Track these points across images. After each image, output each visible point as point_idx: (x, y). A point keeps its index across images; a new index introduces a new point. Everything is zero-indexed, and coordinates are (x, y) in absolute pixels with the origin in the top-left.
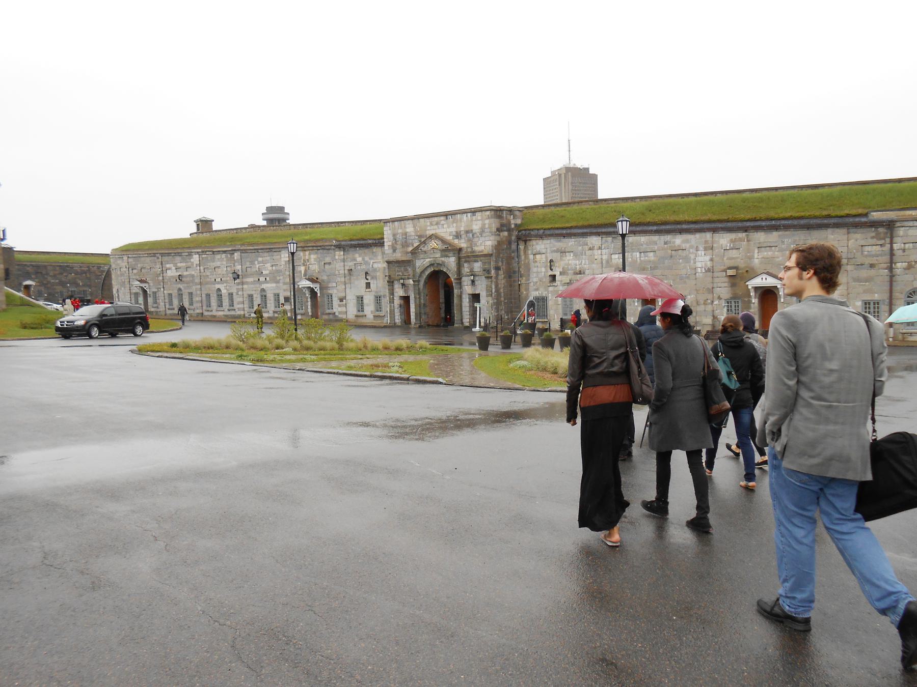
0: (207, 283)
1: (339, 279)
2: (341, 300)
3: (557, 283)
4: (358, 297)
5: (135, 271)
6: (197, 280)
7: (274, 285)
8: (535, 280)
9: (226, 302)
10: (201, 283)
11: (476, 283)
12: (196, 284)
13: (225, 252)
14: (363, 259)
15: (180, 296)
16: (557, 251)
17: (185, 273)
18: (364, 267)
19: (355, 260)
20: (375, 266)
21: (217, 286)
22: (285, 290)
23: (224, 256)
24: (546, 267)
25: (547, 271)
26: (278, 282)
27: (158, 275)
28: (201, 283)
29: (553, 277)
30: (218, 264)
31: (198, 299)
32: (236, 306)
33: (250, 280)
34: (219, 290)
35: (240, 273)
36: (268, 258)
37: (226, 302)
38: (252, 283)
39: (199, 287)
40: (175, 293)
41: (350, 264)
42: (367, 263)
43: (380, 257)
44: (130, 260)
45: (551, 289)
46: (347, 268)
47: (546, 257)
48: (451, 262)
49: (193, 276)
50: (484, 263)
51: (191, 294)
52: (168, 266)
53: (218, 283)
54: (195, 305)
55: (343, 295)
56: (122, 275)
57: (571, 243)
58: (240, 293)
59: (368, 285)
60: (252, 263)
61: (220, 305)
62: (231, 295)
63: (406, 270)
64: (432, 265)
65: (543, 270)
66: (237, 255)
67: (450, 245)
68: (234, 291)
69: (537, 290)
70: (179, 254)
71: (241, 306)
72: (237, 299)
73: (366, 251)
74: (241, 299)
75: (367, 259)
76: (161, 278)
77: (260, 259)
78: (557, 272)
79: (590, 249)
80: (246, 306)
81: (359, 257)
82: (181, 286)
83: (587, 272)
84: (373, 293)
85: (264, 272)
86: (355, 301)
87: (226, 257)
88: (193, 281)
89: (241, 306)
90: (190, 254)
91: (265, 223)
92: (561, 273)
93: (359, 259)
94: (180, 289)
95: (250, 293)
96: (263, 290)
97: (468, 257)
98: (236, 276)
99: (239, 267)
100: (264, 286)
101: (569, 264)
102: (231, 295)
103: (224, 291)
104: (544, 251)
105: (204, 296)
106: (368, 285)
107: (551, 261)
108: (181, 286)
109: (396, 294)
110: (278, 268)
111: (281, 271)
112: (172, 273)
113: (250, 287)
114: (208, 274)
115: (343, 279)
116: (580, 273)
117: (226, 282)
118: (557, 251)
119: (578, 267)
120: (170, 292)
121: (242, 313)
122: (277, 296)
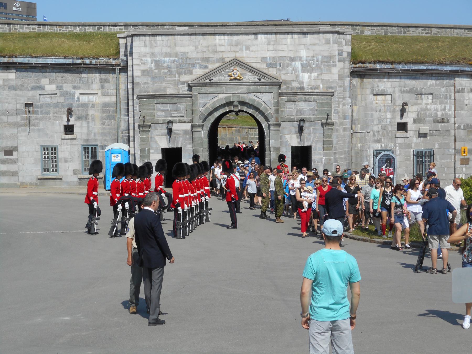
2: (8, 152)
3: (410, 133)
4: (45, 148)
8: (375, 128)
11: (305, 131)
16: (410, 91)
18: (61, 100)
19: (42, 88)
20: (84, 99)
24: (393, 112)
25: (393, 118)
29: (402, 127)
41: (30, 95)
42: (65, 94)
43: (96, 87)
45: (399, 141)
47: (393, 100)
48: (266, 100)
50: (322, 105)
57: (430, 83)
59: (69, 129)
63: (177, 109)
64: (230, 103)
65: (389, 115)
67: (265, 75)
69: (379, 141)
73: (67, 75)
75: (67, 87)
78: (408, 119)
79: (459, 92)
81: (49, 83)
83: (452, 120)
86: (39, 154)
92: (415, 121)
93: (50, 88)
97: (295, 94)
101: (426, 109)
104: (390, 91)
106: (69, 129)
107: (405, 104)
109: (154, 146)
116: (443, 121)
118: (410, 91)
119: (439, 114)
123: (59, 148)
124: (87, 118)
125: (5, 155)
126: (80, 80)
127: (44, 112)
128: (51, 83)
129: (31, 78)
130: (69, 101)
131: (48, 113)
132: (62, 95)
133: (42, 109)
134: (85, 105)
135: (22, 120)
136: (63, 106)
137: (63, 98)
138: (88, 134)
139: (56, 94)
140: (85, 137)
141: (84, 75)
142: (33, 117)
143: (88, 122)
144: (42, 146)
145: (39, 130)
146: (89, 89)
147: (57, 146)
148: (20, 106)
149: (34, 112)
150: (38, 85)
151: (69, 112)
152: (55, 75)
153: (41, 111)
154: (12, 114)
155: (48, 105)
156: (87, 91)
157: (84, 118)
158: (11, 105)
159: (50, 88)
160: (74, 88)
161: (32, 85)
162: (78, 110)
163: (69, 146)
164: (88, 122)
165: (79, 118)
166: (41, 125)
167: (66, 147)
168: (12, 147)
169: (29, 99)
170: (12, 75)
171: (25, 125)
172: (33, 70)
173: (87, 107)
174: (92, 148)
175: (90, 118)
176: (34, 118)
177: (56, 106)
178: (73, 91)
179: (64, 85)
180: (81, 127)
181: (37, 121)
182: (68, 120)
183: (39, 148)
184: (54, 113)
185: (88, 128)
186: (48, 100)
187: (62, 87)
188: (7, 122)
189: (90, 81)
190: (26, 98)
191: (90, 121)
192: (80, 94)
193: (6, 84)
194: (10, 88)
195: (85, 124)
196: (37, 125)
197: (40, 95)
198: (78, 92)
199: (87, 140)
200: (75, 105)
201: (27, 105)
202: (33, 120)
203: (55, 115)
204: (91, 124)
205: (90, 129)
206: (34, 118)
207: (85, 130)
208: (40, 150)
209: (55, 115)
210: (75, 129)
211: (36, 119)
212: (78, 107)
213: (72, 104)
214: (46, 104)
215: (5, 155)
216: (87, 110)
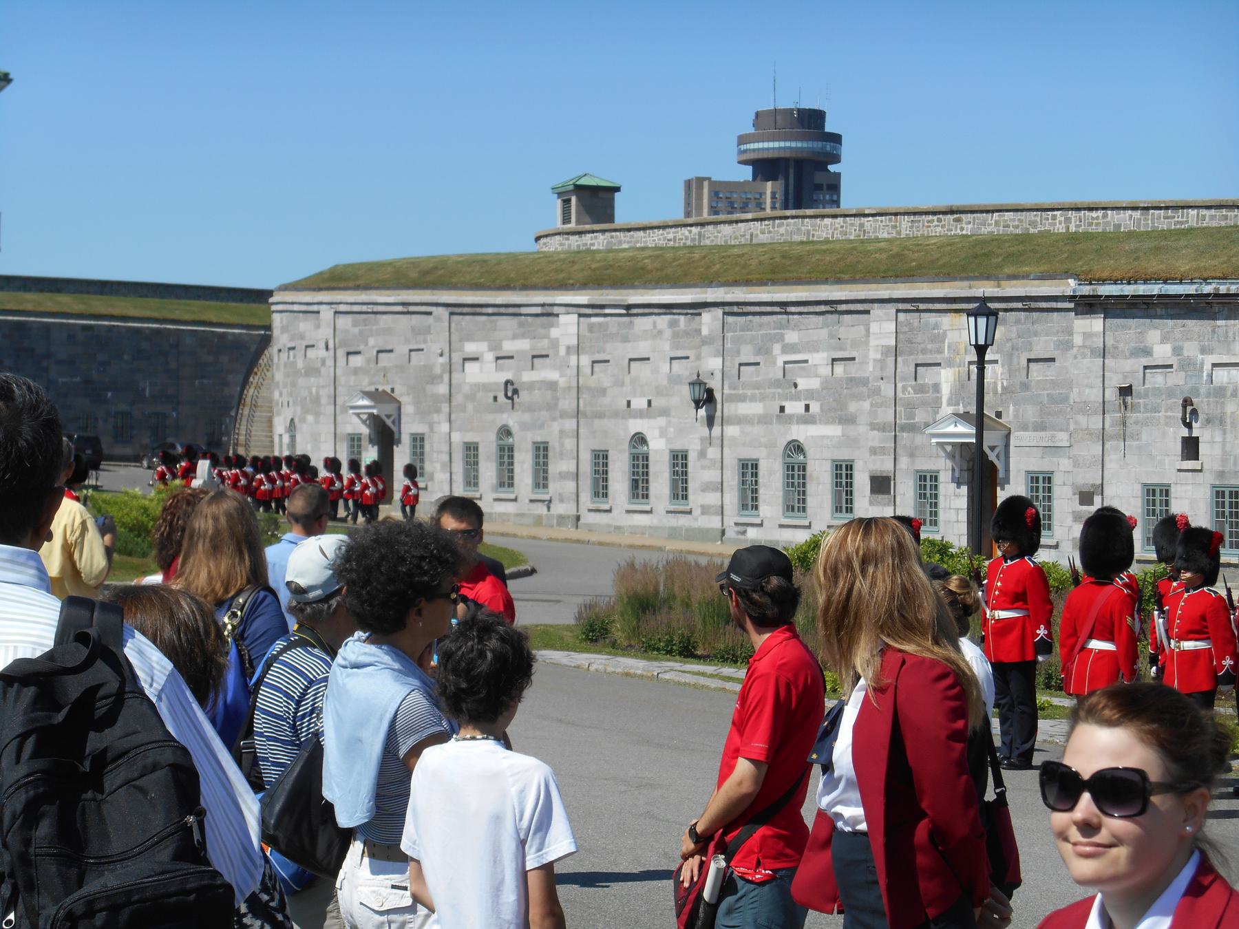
0: (600, 415)
1: (1083, 420)
5: (356, 361)
6: (567, 403)
7: (835, 430)
9: (660, 483)
10: (578, 414)
12: (564, 415)
13: (668, 308)
14: (1177, 351)
15: (506, 455)
17: (527, 377)
18: (1176, 379)
19: (1147, 352)
21: (635, 426)
22: (874, 451)
23: (663, 321)
26: (849, 420)
27: (434, 379)
28: (578, 414)
30: (643, 348)
31: (567, 466)
32: (697, 498)
33: (745, 408)
34: (639, 439)
35: (714, 384)
36: (823, 333)
37: (660, 483)
38: (763, 420)
39: (570, 424)
40: (488, 445)
41: (1124, 369)
42: (1188, 366)
44: (344, 322)
46: (1115, 381)
49: (552, 385)
51: (541, 452)
52: (470, 348)
53: (640, 414)
54: (554, 487)
55: (1090, 478)
56: (311, 371)
58: (713, 453)
59: (1191, 448)
60: (763, 350)
61: (639, 486)
62: (679, 460)
66: (709, 321)
68: (692, 444)
70: (511, 310)
71: (713, 499)
72: (698, 475)
73: (1192, 324)
74: (713, 475)
76: (442, 389)
77: (792, 337)
80: (731, 499)
81: (1159, 339)
82: (511, 419)
84: (1208, 479)
85: (803, 383)
87: (672, 324)
88: (551, 406)
89: (713, 499)
90: (548, 313)
91: (746, 173)
94: (506, 432)
95: (749, 453)
96: (796, 447)
98: (706, 398)
99: (714, 363)
100: (800, 433)
102: (679, 460)
103: (658, 447)
105: (586, 457)
106: (1191, 448)
108: (511, 419)
110: (853, 370)
111: (864, 382)
112: (483, 373)
113: (749, 431)
114: (606, 381)
115: (1096, 423)
117: (665, 412)
120: (471, 437)
121: (714, 522)
122: (843, 473)
123: (1173, 490)
124: (1222, 423)
125: (1082, 503)
126: (1213, 331)
127: (1149, 407)
128: (1164, 340)
129: (1130, 330)
130: (1194, 380)
131: (1156, 410)
132: (1182, 367)
133: (1147, 401)
134: (1220, 392)
135: (1112, 426)
136: (1182, 392)
137: (1182, 374)
138: (1224, 461)
139: (1171, 366)
140: (1217, 467)
141: (1219, 322)
142: (1132, 417)
143: (1224, 432)
144: (1145, 485)
145: (1139, 448)
146: (1229, 352)
147: (1169, 485)
148: (1112, 395)
149: (1135, 408)
150: (1142, 345)
151: (1189, 412)
152: (1170, 322)
153: (1145, 405)
154: (1095, 412)
155: (1157, 392)
156: (1225, 359)
157: (1217, 422)
158: (1095, 390)
159: (1162, 352)
160: (1204, 351)
161: (1132, 345)
162: (1208, 405)
163: (1190, 487)
164: (1224, 432)
165: (1208, 421)
166: (1144, 437)
167: (1185, 488)
168: (1093, 485)
169: (1125, 377)
170: (1096, 323)
171: (1115, 437)
172: (1134, 311)
173: (1224, 396)
174: (1231, 492)
175: (1228, 421)
176: (1132, 421)
177: (1170, 392)
178: (1200, 357)
179: (1186, 345)
180: (1212, 442)
181: (1138, 427)
182: (1189, 426)
183: (1138, 490)
184: (1166, 411)
185: (1224, 443)
186: (1157, 379)
187: (1181, 348)
188: (1087, 429)
189: (1231, 334)
190: (1121, 376)
191: (1228, 427)
192: (1214, 365)
193: (1087, 343)
194: (1093, 352)
195: (1218, 438)
196: (1137, 436)
197: (1146, 368)
198: (1210, 359)
199: (1221, 474)
200: (1203, 390)
201: (1126, 391)
202: (1131, 428)
203: (1169, 414)
204: (1229, 436)
205: (1228, 448)
206: (1132, 421)
207: (1217, 451)
208: (1139, 494)
209: (1169, 414)
210: (1203, 448)
211: (1136, 423)
212: (1208, 395)
213: (1197, 390)
214: (1154, 388)
215: (1082, 503)
216: (1223, 403)
